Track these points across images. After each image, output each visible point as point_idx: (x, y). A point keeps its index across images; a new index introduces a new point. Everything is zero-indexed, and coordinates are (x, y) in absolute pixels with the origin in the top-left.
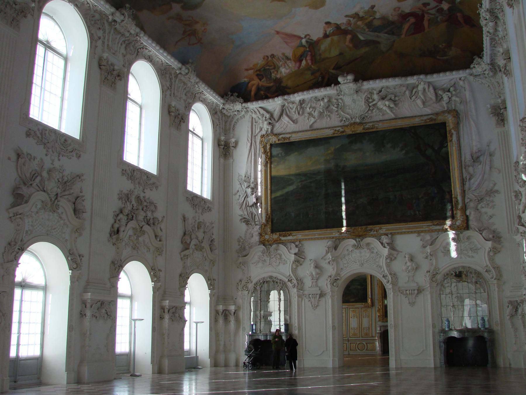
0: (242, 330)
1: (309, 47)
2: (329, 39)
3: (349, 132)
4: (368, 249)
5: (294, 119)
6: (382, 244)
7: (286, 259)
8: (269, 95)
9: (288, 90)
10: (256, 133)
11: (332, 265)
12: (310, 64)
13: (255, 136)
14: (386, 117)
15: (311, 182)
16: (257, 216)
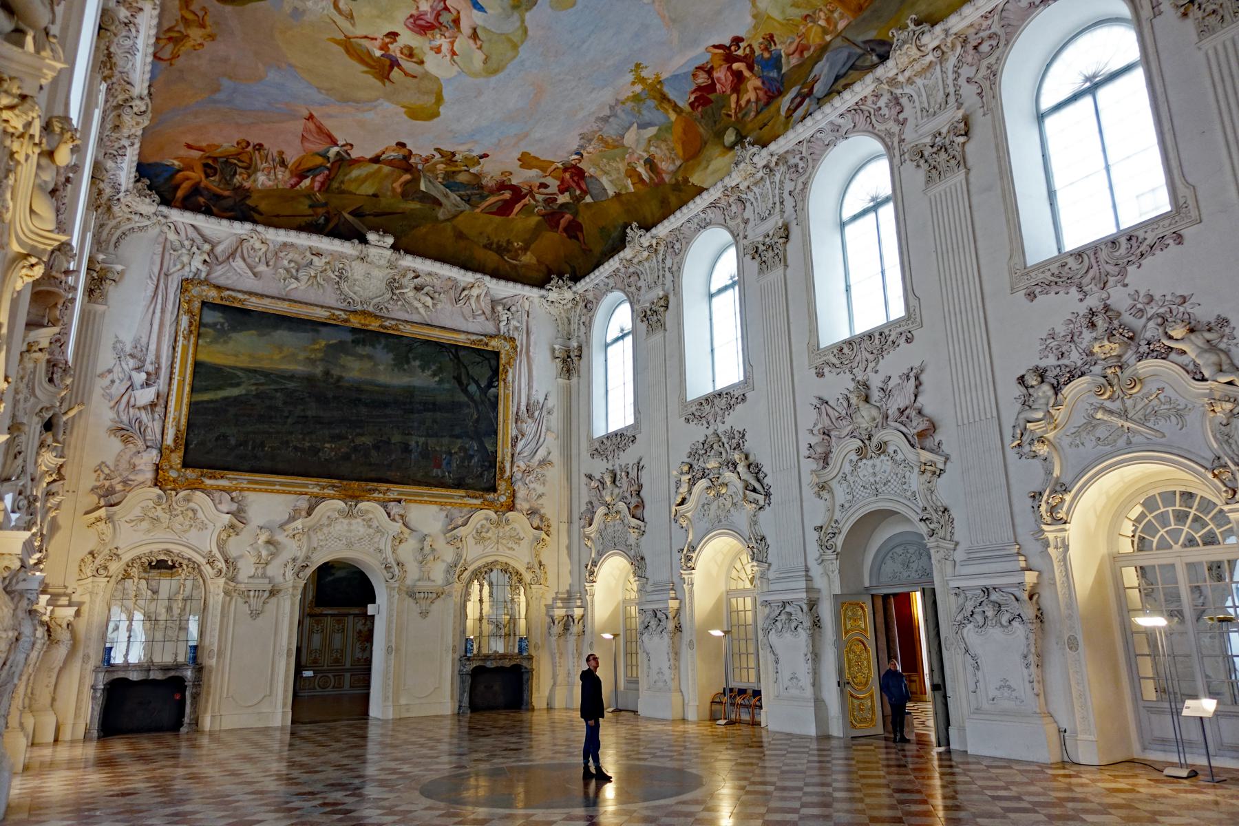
0: (81, 661)
1: (332, 164)
2: (376, 166)
3: (356, 322)
4: (364, 520)
5: (256, 270)
6: (389, 515)
7: (206, 521)
8: (214, 209)
9: (256, 216)
10: (171, 271)
11: (299, 540)
12: (316, 189)
13: (166, 275)
14: (416, 318)
15: (276, 390)
16: (149, 429)
